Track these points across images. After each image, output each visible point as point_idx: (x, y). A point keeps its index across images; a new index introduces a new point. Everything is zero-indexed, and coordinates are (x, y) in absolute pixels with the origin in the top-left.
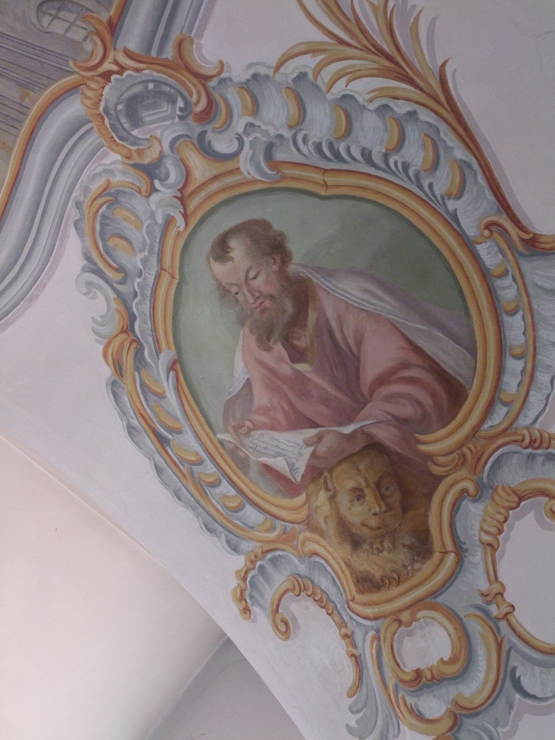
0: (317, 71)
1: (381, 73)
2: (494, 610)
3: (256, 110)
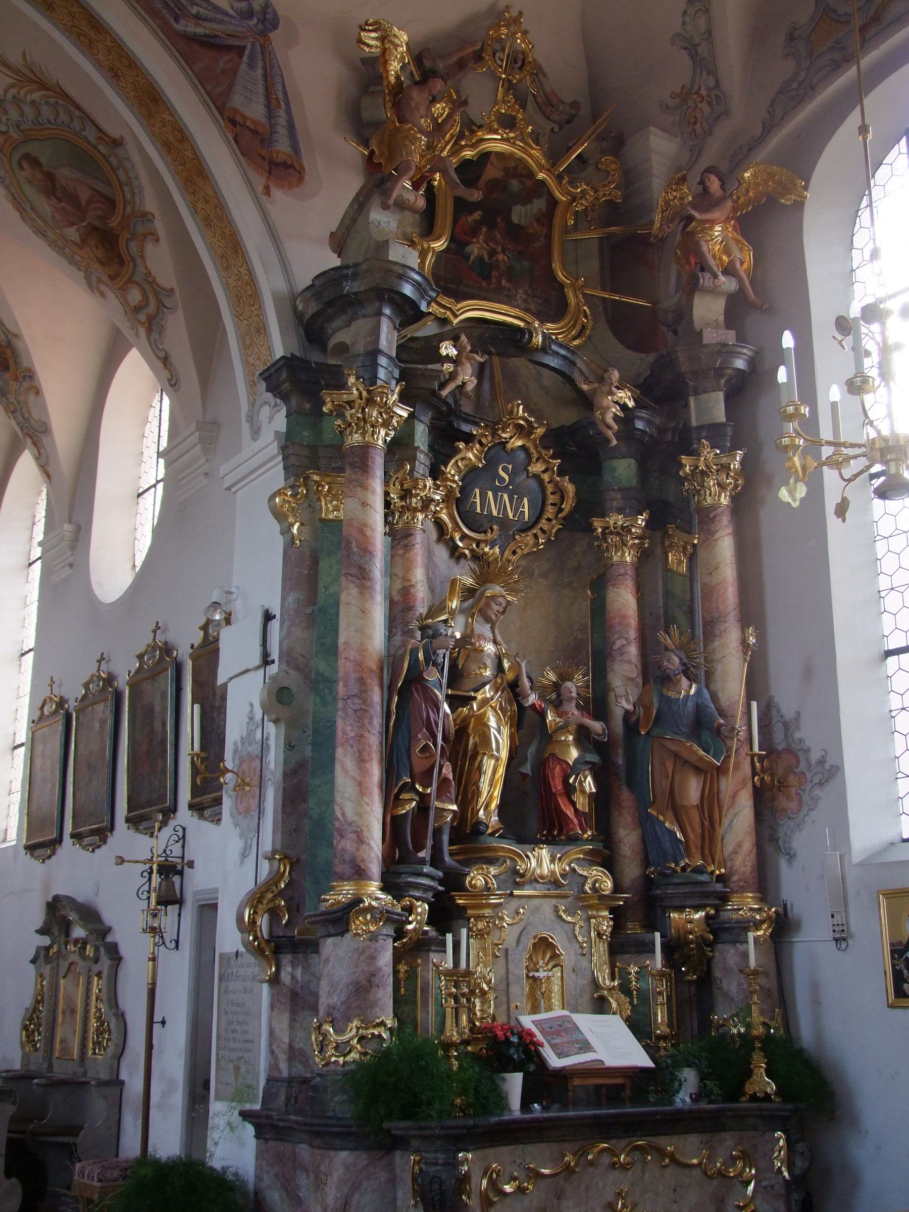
0: (18, 93)
1: (39, 89)
2: (150, 280)
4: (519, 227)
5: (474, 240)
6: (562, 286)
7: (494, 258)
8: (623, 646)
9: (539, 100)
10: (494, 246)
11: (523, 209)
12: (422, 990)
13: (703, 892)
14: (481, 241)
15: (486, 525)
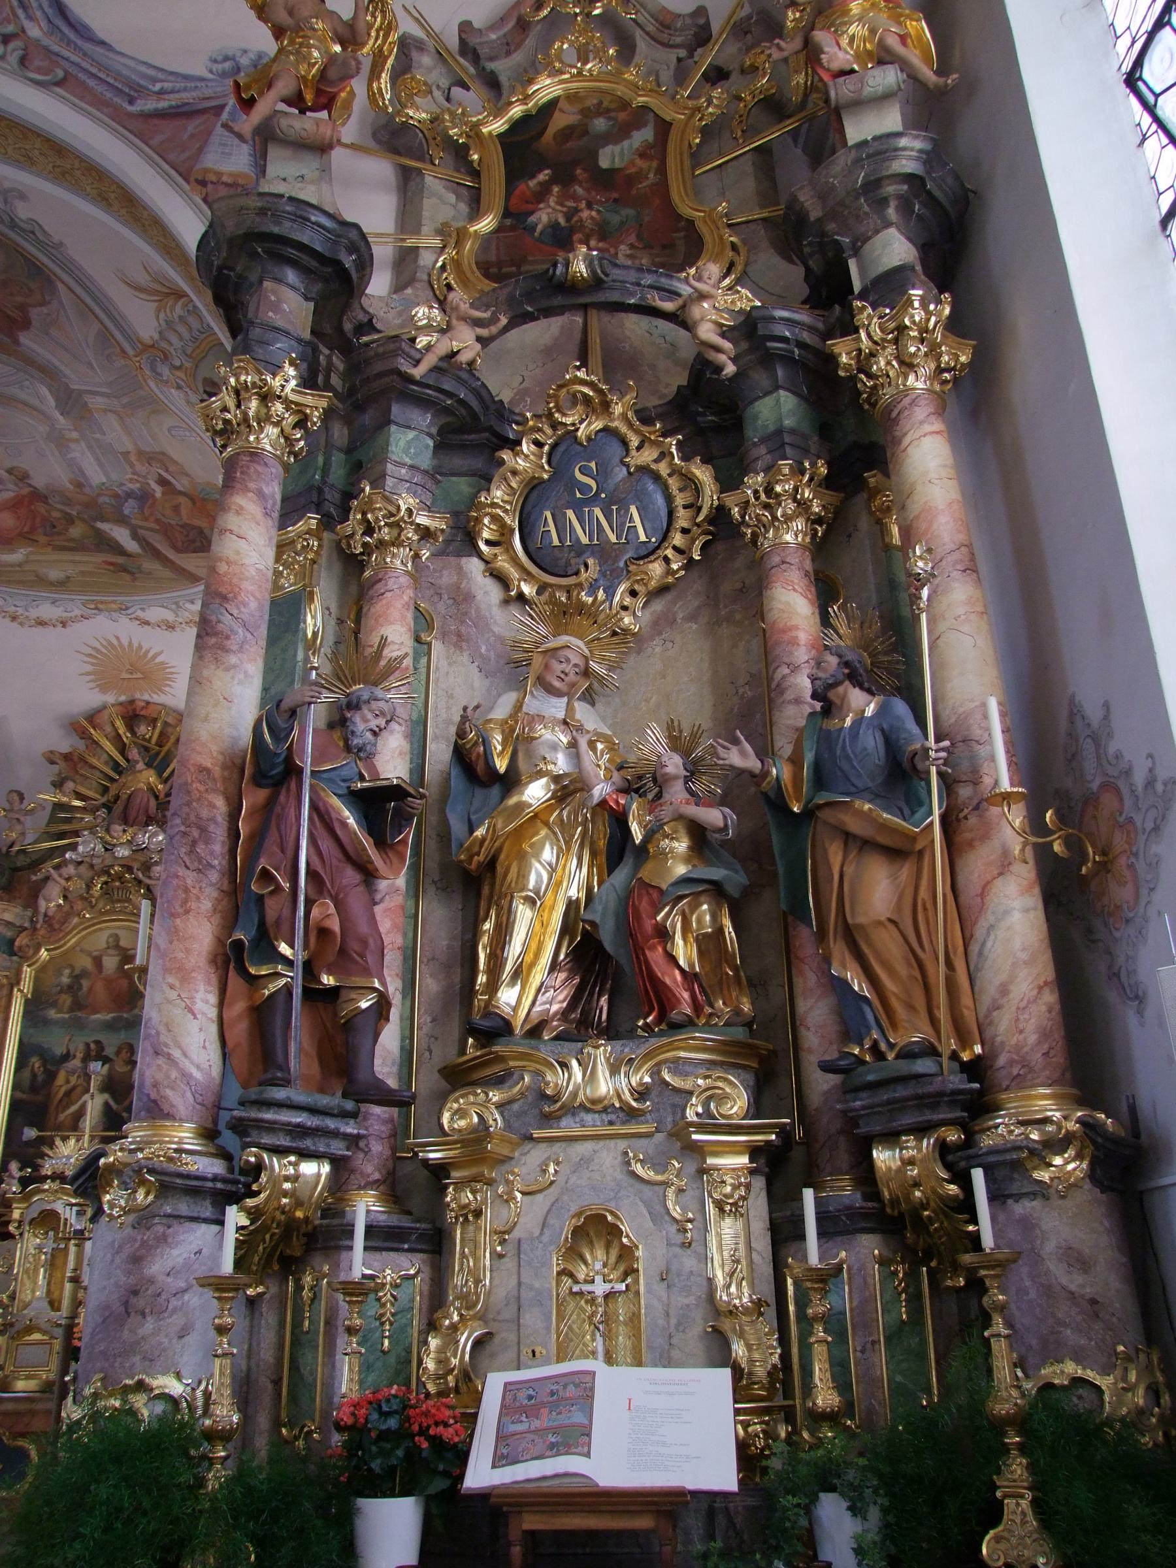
3: (171, 344)
4: (612, 172)
5: (542, 206)
6: (691, 223)
7: (575, 219)
8: (784, 677)
9: (650, 28)
10: (574, 205)
11: (617, 149)
12: (327, 1323)
13: (918, 1097)
14: (552, 204)
15: (573, 561)
